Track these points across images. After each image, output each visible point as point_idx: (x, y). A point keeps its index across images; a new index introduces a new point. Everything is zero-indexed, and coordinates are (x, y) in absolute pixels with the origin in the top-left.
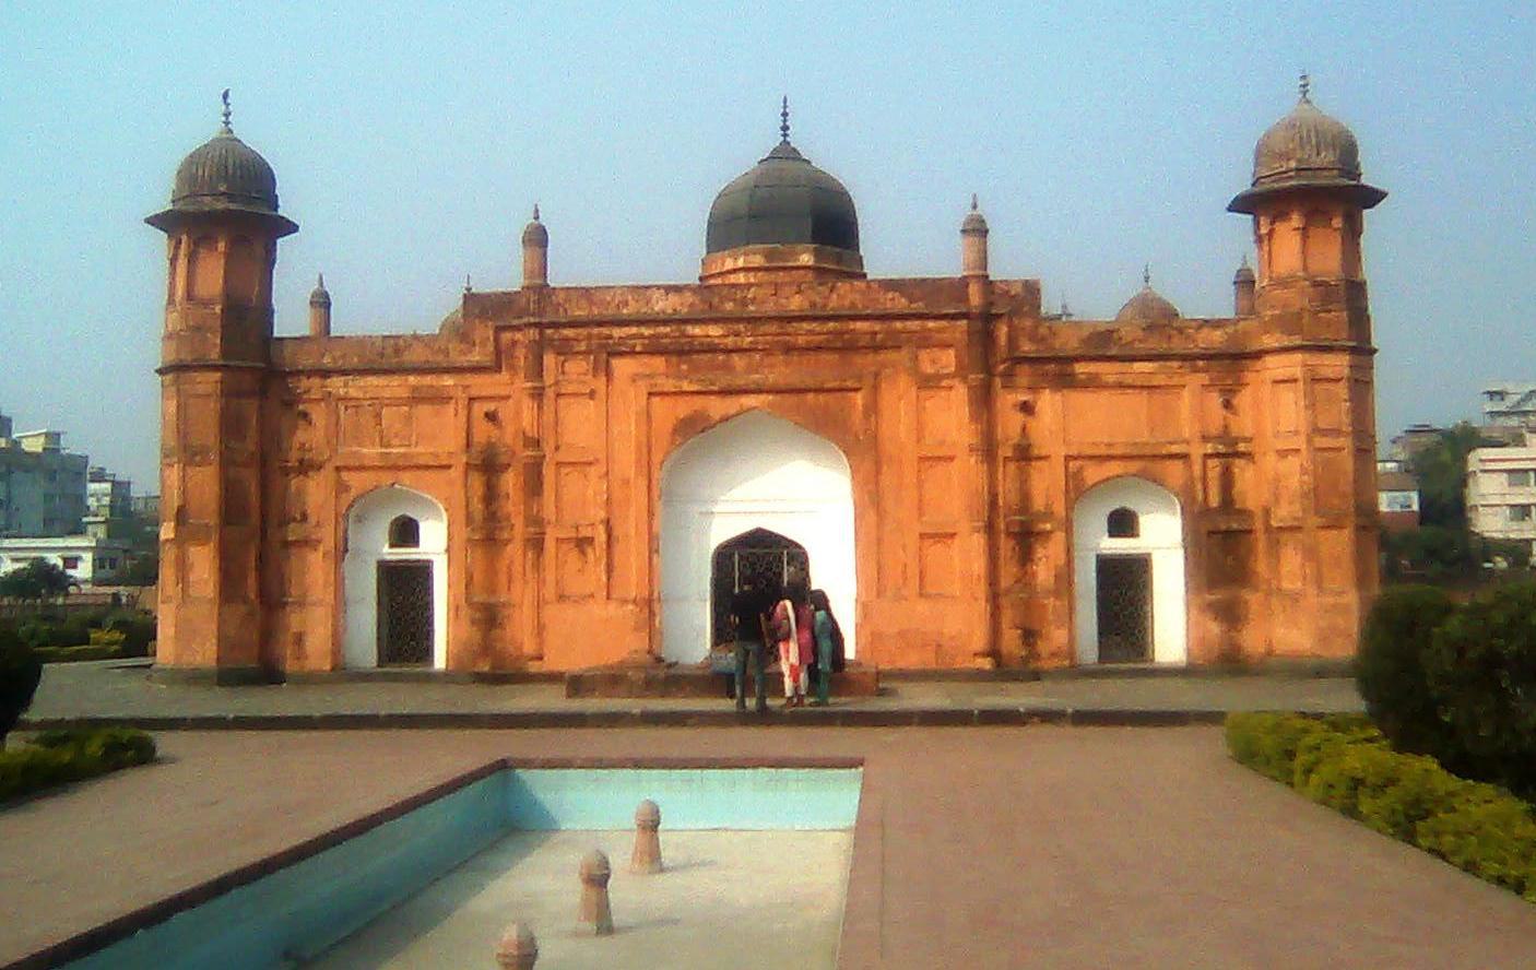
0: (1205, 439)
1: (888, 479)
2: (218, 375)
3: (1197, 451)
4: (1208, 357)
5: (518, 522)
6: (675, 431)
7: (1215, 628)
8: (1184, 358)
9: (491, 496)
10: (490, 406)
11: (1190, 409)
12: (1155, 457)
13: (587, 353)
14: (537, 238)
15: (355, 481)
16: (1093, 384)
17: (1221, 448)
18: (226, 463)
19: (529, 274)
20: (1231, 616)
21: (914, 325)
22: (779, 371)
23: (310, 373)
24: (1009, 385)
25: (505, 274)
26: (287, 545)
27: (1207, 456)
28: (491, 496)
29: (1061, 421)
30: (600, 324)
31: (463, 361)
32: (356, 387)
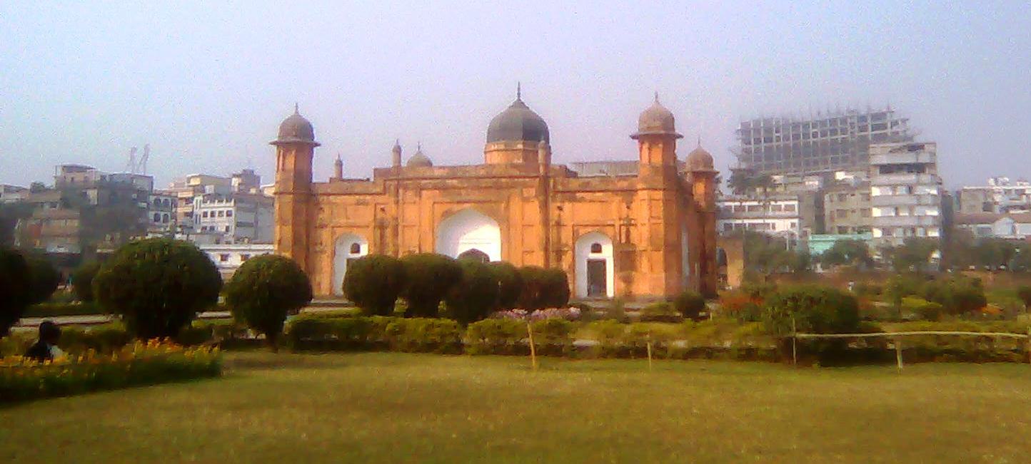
0: (620, 219)
1: (512, 231)
2: (291, 196)
3: (617, 224)
4: (622, 191)
5: (391, 245)
6: (443, 216)
7: (623, 285)
8: (613, 191)
9: (382, 237)
10: (382, 206)
11: (614, 209)
12: (604, 226)
13: (412, 189)
14: (398, 150)
15: (338, 231)
16: (582, 200)
17: (625, 222)
18: (294, 225)
19: (395, 162)
20: (628, 281)
21: (521, 180)
22: (476, 196)
23: (324, 194)
24: (554, 200)
25: (388, 163)
26: (316, 252)
27: (620, 226)
28: (382, 237)
29: (573, 213)
30: (418, 179)
31: (374, 191)
32: (339, 199)
